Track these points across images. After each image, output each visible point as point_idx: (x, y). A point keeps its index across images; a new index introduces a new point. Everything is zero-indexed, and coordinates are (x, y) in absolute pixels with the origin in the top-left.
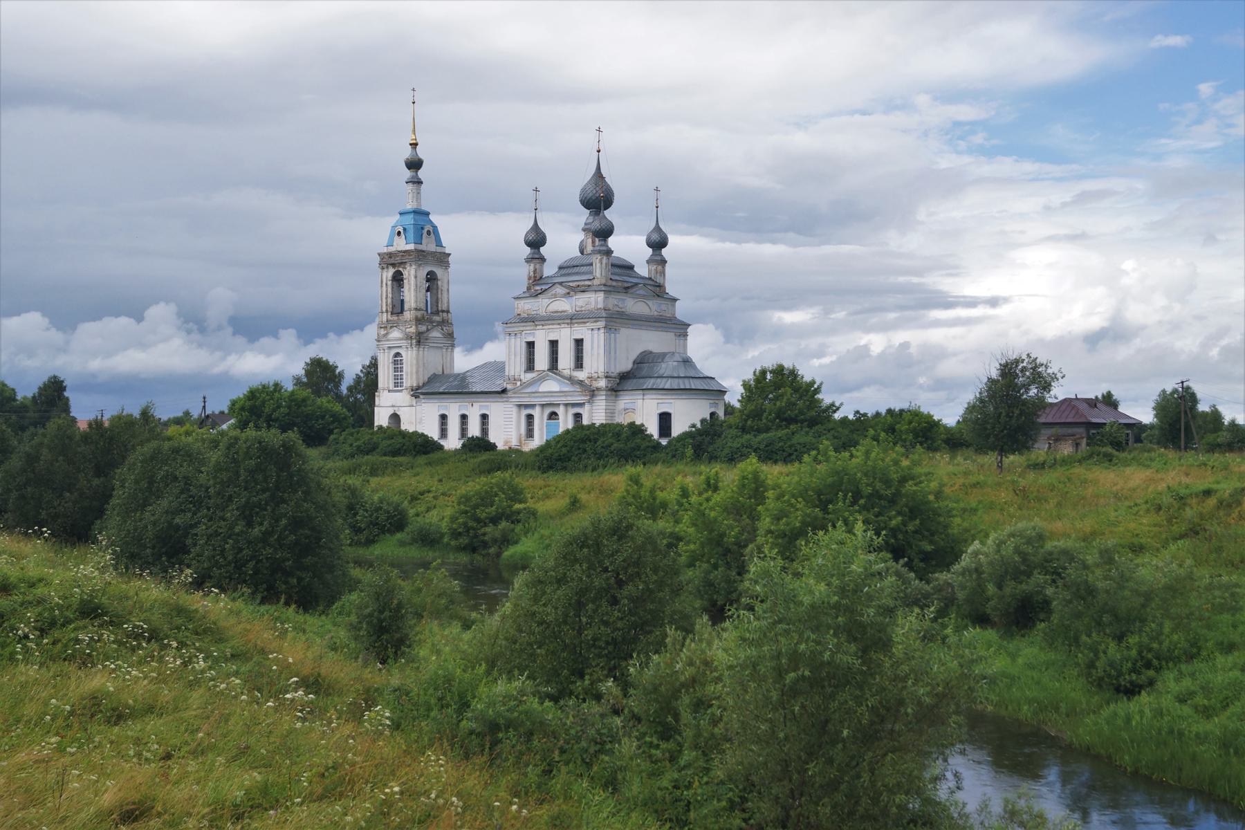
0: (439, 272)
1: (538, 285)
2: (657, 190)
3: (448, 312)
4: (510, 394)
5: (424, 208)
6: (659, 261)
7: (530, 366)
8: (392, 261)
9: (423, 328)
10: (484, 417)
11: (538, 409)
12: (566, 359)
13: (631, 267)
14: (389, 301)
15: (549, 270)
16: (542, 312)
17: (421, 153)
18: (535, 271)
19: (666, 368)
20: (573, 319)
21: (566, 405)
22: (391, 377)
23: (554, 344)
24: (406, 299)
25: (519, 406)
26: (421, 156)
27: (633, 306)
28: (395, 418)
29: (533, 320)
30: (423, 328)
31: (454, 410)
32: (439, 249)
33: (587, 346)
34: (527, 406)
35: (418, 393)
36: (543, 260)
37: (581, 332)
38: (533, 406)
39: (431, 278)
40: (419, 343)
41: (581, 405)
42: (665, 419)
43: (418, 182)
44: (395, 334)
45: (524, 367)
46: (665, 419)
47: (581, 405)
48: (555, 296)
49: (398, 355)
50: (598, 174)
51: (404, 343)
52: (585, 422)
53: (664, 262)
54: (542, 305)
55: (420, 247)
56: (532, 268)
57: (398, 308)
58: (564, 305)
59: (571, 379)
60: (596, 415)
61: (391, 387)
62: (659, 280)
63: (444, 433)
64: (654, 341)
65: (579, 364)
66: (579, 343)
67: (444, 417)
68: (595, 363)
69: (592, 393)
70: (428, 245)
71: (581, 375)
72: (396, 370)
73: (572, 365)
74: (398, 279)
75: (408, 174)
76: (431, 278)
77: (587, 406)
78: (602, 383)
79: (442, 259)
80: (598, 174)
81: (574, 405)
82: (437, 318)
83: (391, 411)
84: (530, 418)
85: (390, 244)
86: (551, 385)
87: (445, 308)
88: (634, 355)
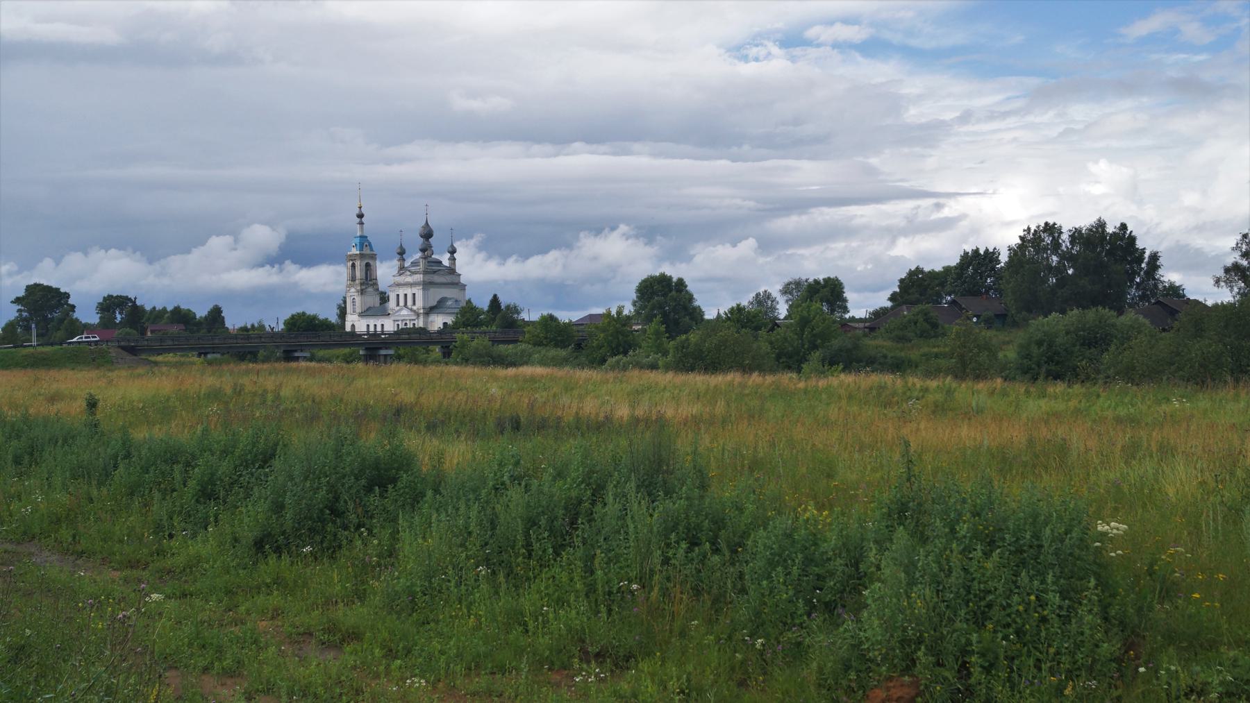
0: (371, 262)
6: (453, 259)
19: (449, 303)
20: (411, 285)
27: (437, 278)
28: (353, 326)
35: (362, 315)
39: (368, 265)
43: (361, 223)
54: (401, 279)
57: (353, 279)
58: (409, 279)
69: (418, 315)
70: (367, 251)
76: (368, 265)
88: (438, 298)
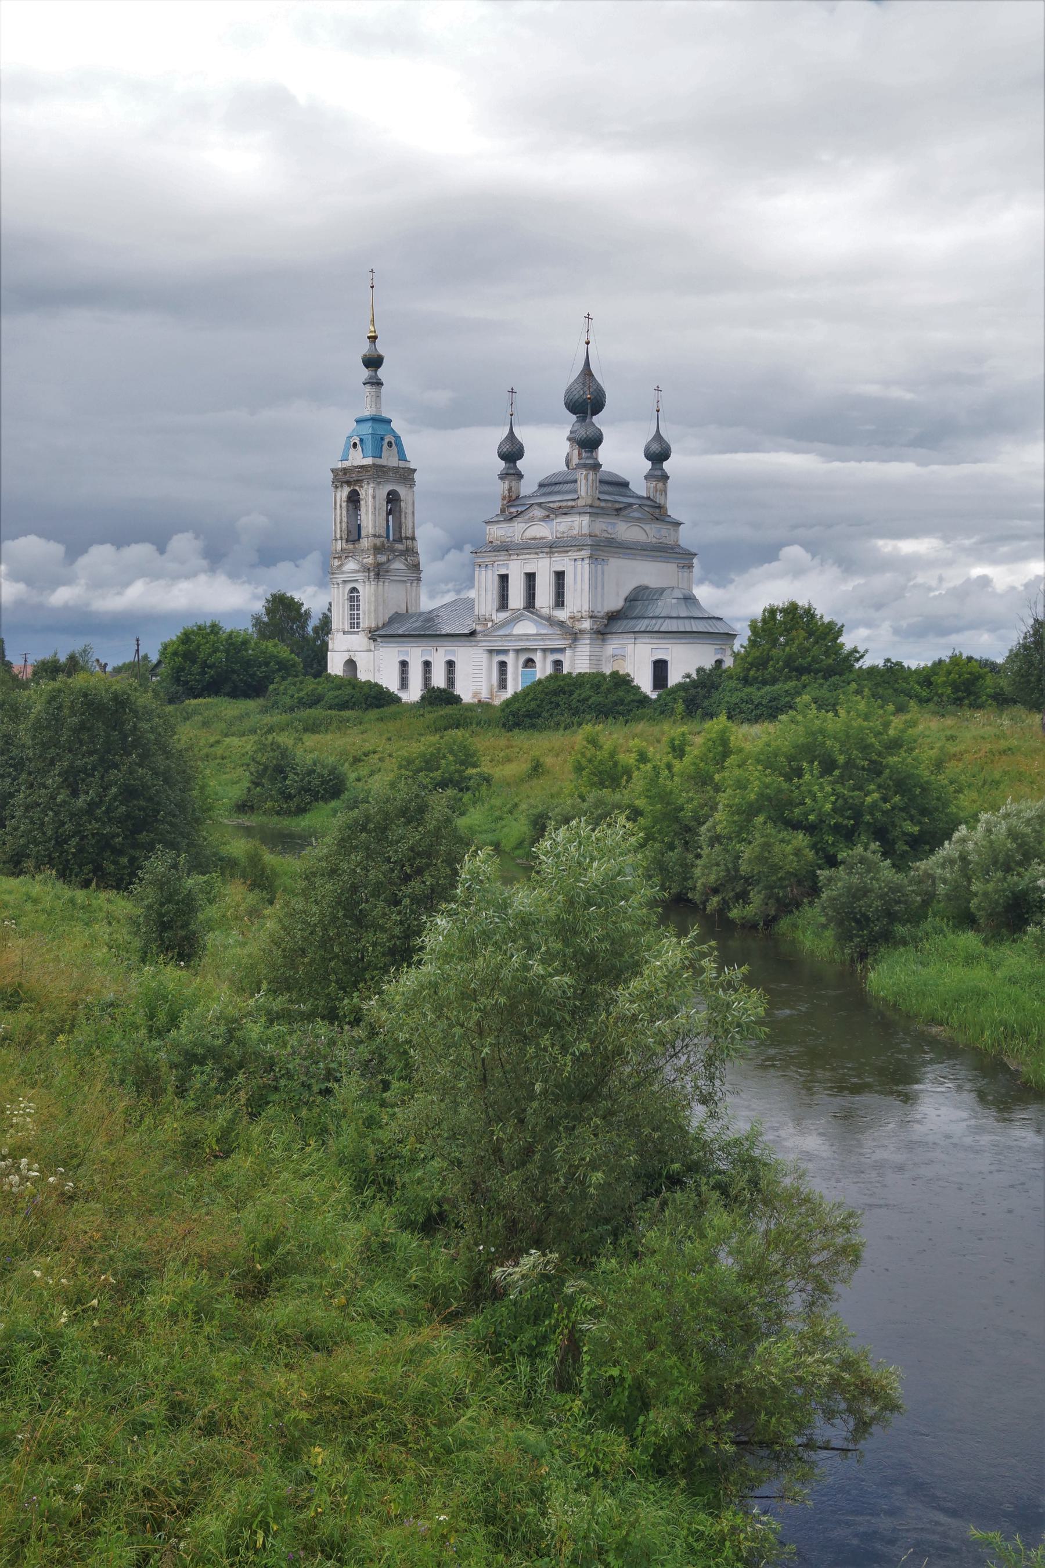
0: (402, 491)
1: (513, 507)
2: (658, 389)
3: (413, 539)
4: (479, 637)
5: (385, 414)
7: (503, 605)
8: (347, 478)
9: (382, 558)
10: (450, 664)
11: (512, 655)
12: (544, 597)
13: (625, 485)
14: (344, 526)
15: (527, 487)
17: (381, 349)
18: (510, 490)
19: (662, 607)
20: (552, 547)
21: (544, 650)
23: (531, 577)
24: (364, 524)
25: (491, 651)
26: (381, 351)
28: (351, 665)
29: (506, 549)
30: (382, 558)
31: (415, 655)
32: (402, 464)
33: (568, 580)
34: (499, 652)
35: (378, 635)
36: (519, 476)
38: (505, 652)
39: (393, 498)
40: (378, 576)
41: (561, 650)
42: (660, 668)
43: (376, 383)
44: (351, 565)
45: (496, 605)
46: (660, 668)
48: (533, 519)
49: (354, 590)
50: (587, 371)
51: (360, 576)
53: (665, 478)
54: (517, 531)
55: (379, 461)
56: (506, 486)
57: (354, 534)
58: (542, 531)
59: (550, 620)
60: (579, 662)
61: (347, 628)
62: (660, 500)
63: (404, 684)
64: (649, 573)
65: (559, 601)
66: (560, 576)
67: (404, 664)
69: (575, 636)
70: (389, 459)
71: (562, 615)
72: (352, 608)
73: (552, 603)
74: (354, 500)
75: (365, 373)
76: (393, 498)
77: (568, 652)
79: (406, 475)
80: (587, 371)
81: (554, 651)
82: (399, 547)
83: (346, 657)
84: (503, 665)
86: (527, 627)
88: (625, 592)
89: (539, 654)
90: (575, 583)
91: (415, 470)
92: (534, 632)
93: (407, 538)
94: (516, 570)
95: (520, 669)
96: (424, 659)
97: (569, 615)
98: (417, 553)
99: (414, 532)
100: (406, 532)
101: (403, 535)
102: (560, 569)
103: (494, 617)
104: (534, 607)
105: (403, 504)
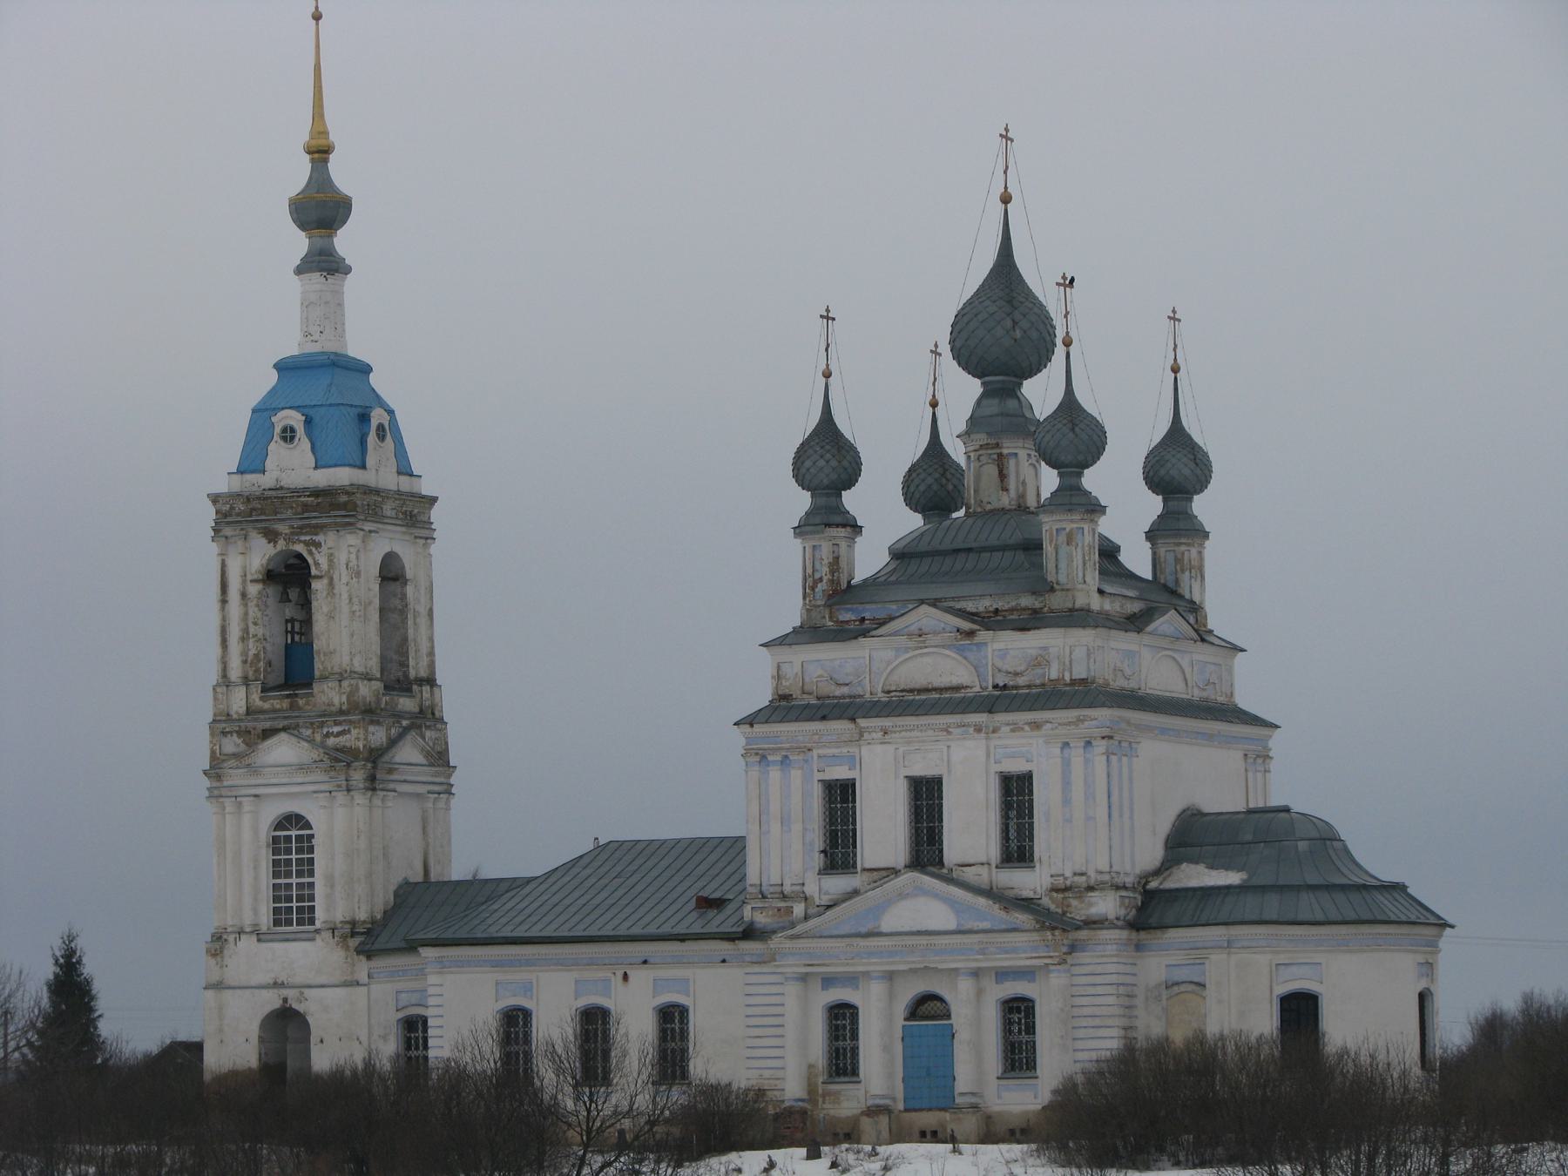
0: (408, 554)
1: (838, 609)
3: (430, 681)
5: (355, 350)
11: (877, 989)
12: (970, 831)
16: (872, 687)
17: (342, 173)
18: (835, 564)
21: (976, 973)
22: (266, 893)
32: (405, 484)
33: (1044, 796)
37: (1030, 746)
39: (391, 574)
40: (372, 784)
43: (324, 263)
44: (283, 751)
45: (818, 860)
47: (1027, 974)
50: (1005, 267)
52: (440, 1048)
58: (944, 667)
61: (265, 919)
65: (1017, 850)
68: (1063, 847)
72: (279, 869)
73: (994, 851)
74: (291, 578)
76: (391, 574)
78: (1106, 905)
79: (414, 512)
80: (1005, 267)
81: (1002, 975)
83: (271, 1001)
85: (252, 462)
87: (423, 674)
89: (965, 986)
90: (1067, 801)
91: (434, 500)
92: (952, 926)
93: (421, 681)
94: (882, 770)
95: (900, 1021)
96: (583, 1002)
97: (1047, 882)
98: (441, 720)
99: (432, 665)
100: (417, 668)
101: (412, 674)
102: (1016, 767)
103: (811, 889)
104: (941, 863)
105: (409, 589)
